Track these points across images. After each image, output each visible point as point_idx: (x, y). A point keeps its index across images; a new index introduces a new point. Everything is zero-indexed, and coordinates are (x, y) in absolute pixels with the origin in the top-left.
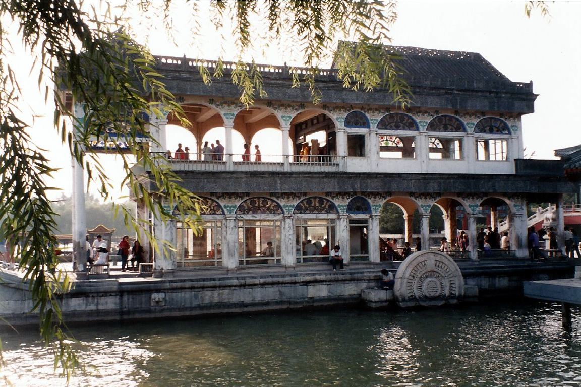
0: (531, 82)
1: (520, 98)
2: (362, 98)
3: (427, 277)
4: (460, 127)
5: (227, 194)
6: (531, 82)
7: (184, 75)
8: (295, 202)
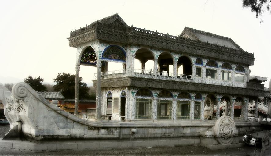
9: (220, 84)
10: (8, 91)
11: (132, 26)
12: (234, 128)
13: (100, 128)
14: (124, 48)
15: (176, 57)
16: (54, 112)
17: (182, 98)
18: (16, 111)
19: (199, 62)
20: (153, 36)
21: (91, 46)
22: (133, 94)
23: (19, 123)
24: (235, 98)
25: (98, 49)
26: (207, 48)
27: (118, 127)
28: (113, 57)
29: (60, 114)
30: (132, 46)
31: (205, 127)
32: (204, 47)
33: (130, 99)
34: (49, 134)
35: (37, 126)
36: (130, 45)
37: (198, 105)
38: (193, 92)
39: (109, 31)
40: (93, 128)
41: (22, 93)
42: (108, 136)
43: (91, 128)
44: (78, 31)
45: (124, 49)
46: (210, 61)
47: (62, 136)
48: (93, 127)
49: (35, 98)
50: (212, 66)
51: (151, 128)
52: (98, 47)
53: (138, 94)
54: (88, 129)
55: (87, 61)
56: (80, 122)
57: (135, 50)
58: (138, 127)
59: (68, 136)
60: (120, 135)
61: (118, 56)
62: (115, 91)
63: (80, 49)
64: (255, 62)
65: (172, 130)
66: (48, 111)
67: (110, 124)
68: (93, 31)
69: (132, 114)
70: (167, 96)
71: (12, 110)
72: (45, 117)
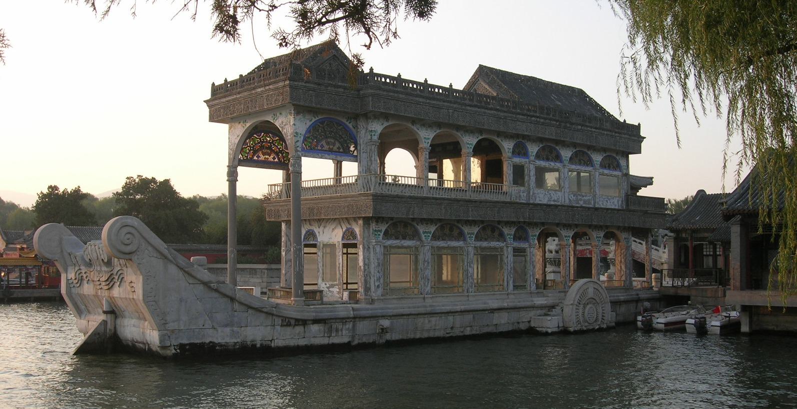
0: (639, 124)
1: (629, 138)
2: (530, 129)
3: (588, 304)
4: (589, 162)
5: (424, 219)
6: (639, 124)
7: (401, 96)
8: (475, 230)
9: (567, 203)
10: (70, 236)
12: (608, 307)
13: (309, 320)
14: (350, 123)
15: (469, 141)
16: (201, 287)
17: (486, 240)
18: (98, 287)
19: (520, 150)
20: (418, 92)
21: (269, 118)
23: (109, 316)
24: (602, 234)
25: (289, 125)
26: (538, 117)
27: (348, 318)
28: (326, 147)
29: (216, 291)
30: (370, 118)
31: (541, 307)
32: (532, 114)
33: (369, 248)
34: (192, 341)
35: (163, 322)
36: (367, 116)
37: (518, 252)
38: (509, 223)
39: (319, 84)
40: (293, 322)
41: (127, 242)
42: (325, 341)
43: (287, 322)
44: (234, 83)
45: (350, 126)
46: (543, 149)
47: (220, 345)
48: (292, 318)
50: (548, 159)
51: (422, 316)
52: (292, 124)
53: (387, 234)
54: (282, 326)
55: (253, 156)
56: (263, 310)
57: (378, 127)
58: (393, 316)
59: (235, 343)
60: (353, 337)
61: (338, 145)
62: (326, 230)
63: (239, 126)
64: (644, 145)
65: (469, 317)
66: (190, 284)
67: (331, 312)
68: (281, 84)
69: (377, 284)
70: (451, 237)
71: (85, 282)
72: (181, 300)
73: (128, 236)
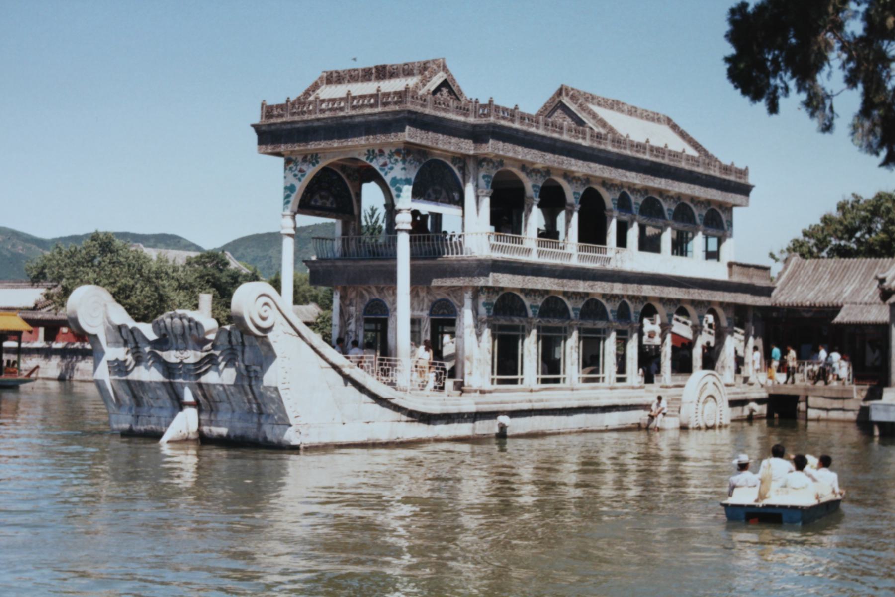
0: (747, 168)
6: (747, 168)
11: (491, 102)
21: (364, 158)
22: (488, 311)
49: (295, 333)
56: (393, 401)
73: (266, 308)
